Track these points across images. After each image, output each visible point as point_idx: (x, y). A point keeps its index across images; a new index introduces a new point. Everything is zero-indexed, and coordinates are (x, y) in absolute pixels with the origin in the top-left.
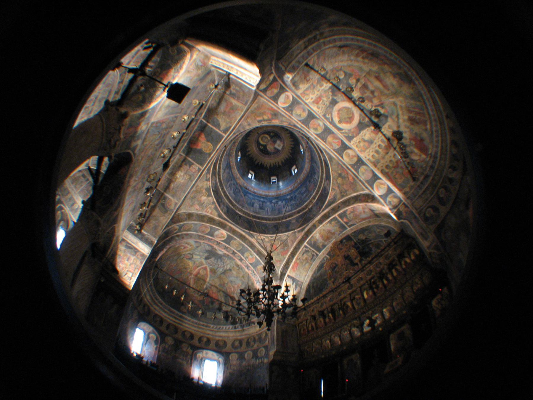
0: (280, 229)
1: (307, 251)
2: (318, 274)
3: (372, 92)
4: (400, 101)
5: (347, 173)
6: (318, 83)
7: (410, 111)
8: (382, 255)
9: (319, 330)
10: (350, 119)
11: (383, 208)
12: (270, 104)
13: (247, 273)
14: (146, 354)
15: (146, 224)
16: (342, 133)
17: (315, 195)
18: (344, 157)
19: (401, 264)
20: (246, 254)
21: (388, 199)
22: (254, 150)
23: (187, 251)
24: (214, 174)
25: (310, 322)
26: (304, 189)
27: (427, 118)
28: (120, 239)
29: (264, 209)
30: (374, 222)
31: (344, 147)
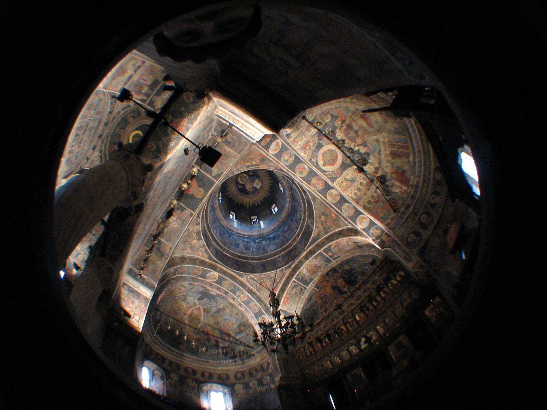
0: (267, 267)
1: (296, 286)
2: (309, 305)
8: (369, 281)
11: (367, 239)
12: (260, 151)
13: (240, 310)
18: (328, 197)
20: (238, 293)
21: (371, 231)
25: (307, 349)
31: (328, 187)
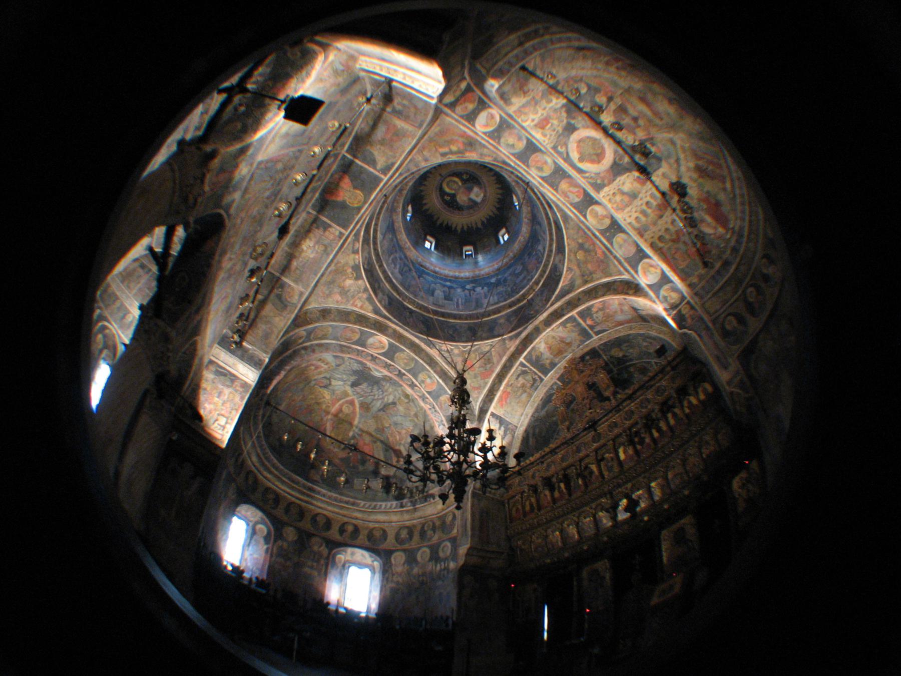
0: (479, 334)
2: (543, 413)
3: (635, 119)
4: (680, 138)
5: (594, 244)
6: (542, 97)
7: (696, 156)
8: (651, 387)
9: (542, 512)
10: (598, 157)
11: (654, 306)
12: (462, 127)
14: (249, 564)
15: (250, 331)
16: (584, 178)
17: (538, 277)
18: (588, 217)
19: (682, 407)
21: (663, 292)
22: (433, 202)
23: (320, 373)
24: (366, 241)
25: (528, 496)
26: (519, 268)
27: (725, 172)
28: (206, 361)
29: (452, 300)
30: (638, 329)
31: (589, 201)
